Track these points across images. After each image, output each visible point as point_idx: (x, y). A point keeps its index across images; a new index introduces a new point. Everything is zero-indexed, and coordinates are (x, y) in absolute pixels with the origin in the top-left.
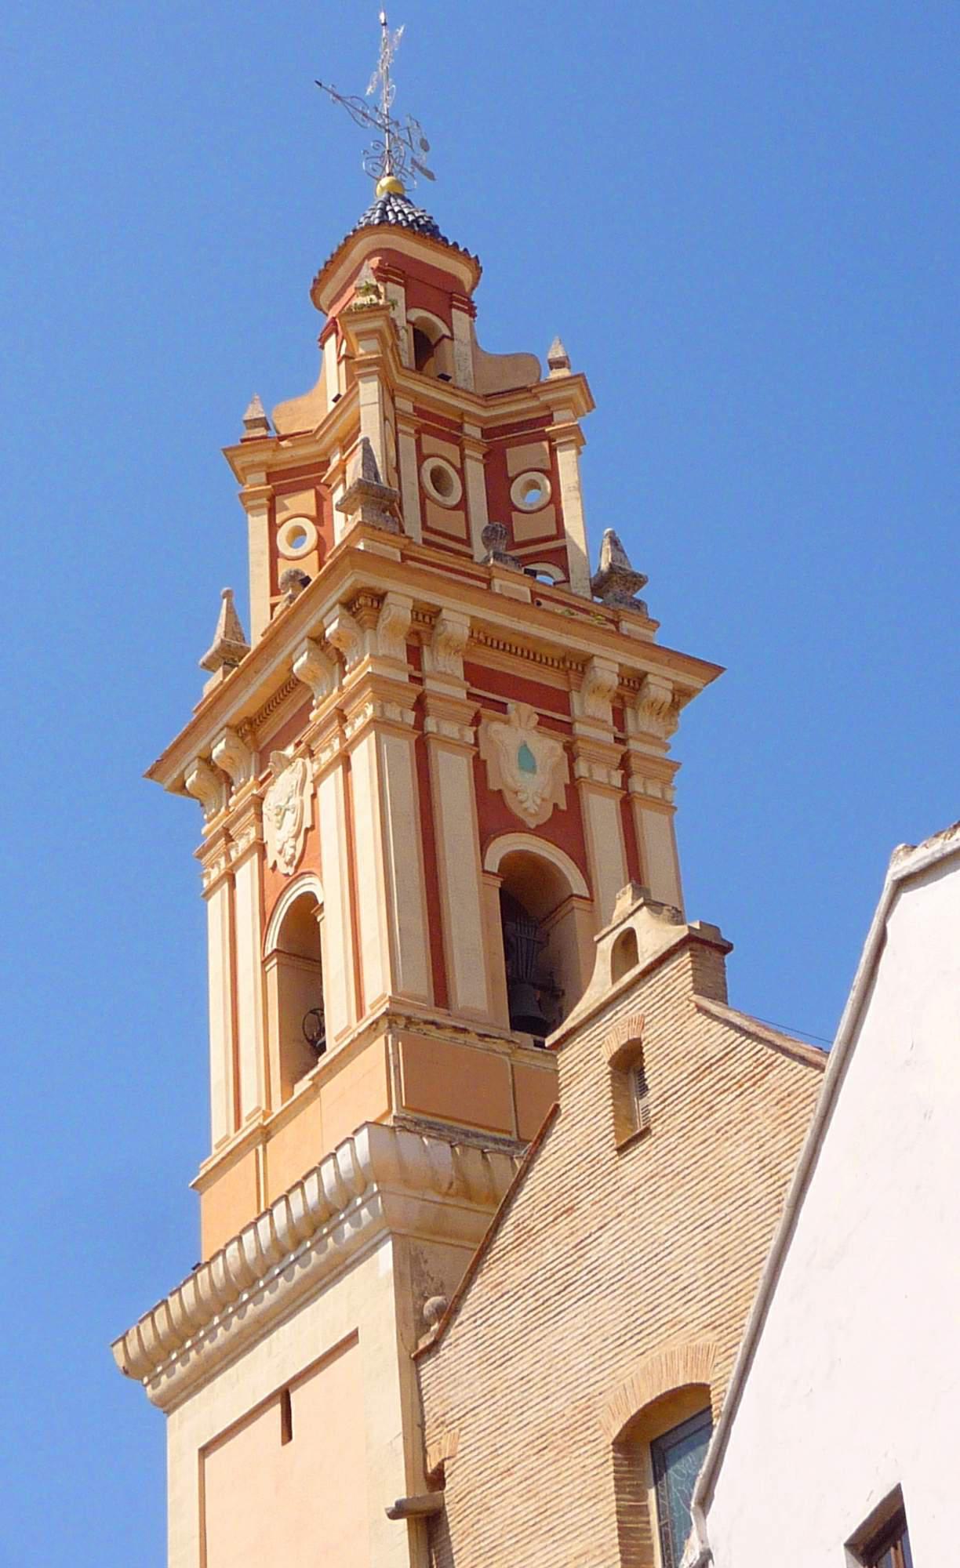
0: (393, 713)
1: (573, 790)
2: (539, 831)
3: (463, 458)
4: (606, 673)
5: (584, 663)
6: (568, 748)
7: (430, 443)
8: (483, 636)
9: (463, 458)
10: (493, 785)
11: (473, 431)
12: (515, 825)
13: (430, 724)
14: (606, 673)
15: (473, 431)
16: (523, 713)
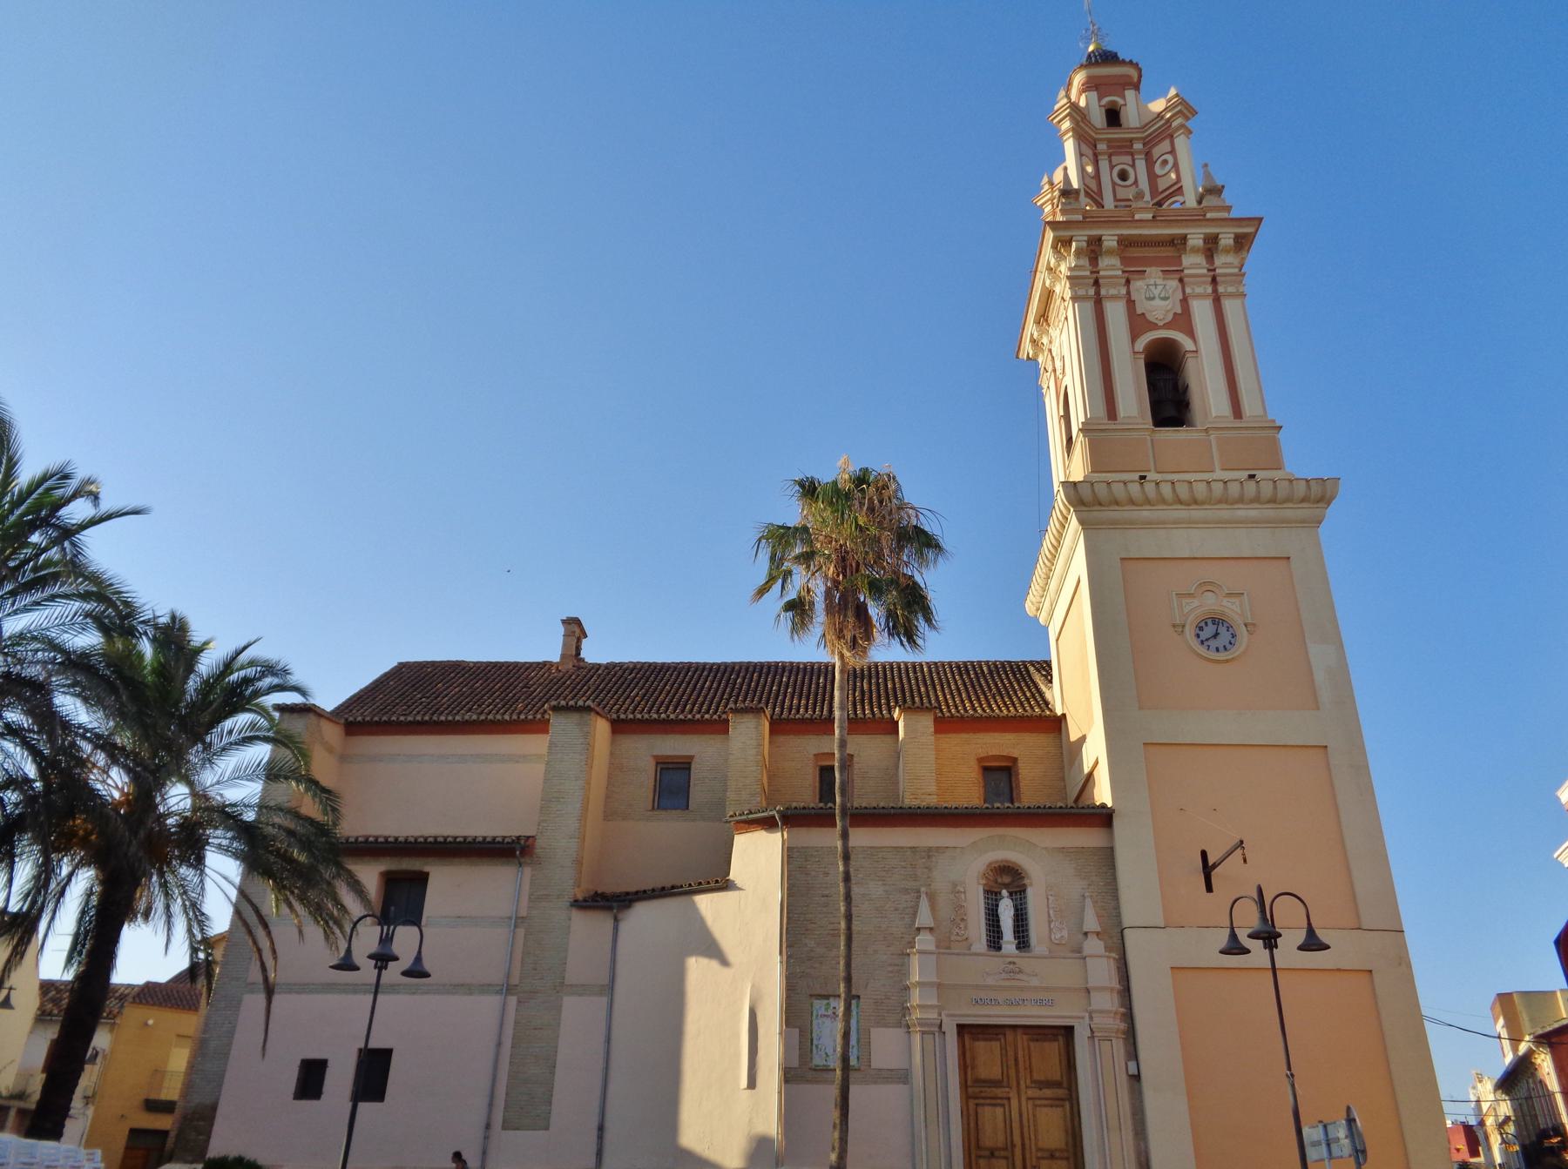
0: (1081, 292)
1: (1185, 301)
2: (1167, 326)
4: (1196, 239)
5: (1184, 238)
6: (1181, 280)
7: (1115, 159)
8: (1126, 243)
10: (1139, 311)
11: (1138, 146)
12: (1154, 326)
13: (1103, 292)
14: (1196, 239)
15: (1138, 146)
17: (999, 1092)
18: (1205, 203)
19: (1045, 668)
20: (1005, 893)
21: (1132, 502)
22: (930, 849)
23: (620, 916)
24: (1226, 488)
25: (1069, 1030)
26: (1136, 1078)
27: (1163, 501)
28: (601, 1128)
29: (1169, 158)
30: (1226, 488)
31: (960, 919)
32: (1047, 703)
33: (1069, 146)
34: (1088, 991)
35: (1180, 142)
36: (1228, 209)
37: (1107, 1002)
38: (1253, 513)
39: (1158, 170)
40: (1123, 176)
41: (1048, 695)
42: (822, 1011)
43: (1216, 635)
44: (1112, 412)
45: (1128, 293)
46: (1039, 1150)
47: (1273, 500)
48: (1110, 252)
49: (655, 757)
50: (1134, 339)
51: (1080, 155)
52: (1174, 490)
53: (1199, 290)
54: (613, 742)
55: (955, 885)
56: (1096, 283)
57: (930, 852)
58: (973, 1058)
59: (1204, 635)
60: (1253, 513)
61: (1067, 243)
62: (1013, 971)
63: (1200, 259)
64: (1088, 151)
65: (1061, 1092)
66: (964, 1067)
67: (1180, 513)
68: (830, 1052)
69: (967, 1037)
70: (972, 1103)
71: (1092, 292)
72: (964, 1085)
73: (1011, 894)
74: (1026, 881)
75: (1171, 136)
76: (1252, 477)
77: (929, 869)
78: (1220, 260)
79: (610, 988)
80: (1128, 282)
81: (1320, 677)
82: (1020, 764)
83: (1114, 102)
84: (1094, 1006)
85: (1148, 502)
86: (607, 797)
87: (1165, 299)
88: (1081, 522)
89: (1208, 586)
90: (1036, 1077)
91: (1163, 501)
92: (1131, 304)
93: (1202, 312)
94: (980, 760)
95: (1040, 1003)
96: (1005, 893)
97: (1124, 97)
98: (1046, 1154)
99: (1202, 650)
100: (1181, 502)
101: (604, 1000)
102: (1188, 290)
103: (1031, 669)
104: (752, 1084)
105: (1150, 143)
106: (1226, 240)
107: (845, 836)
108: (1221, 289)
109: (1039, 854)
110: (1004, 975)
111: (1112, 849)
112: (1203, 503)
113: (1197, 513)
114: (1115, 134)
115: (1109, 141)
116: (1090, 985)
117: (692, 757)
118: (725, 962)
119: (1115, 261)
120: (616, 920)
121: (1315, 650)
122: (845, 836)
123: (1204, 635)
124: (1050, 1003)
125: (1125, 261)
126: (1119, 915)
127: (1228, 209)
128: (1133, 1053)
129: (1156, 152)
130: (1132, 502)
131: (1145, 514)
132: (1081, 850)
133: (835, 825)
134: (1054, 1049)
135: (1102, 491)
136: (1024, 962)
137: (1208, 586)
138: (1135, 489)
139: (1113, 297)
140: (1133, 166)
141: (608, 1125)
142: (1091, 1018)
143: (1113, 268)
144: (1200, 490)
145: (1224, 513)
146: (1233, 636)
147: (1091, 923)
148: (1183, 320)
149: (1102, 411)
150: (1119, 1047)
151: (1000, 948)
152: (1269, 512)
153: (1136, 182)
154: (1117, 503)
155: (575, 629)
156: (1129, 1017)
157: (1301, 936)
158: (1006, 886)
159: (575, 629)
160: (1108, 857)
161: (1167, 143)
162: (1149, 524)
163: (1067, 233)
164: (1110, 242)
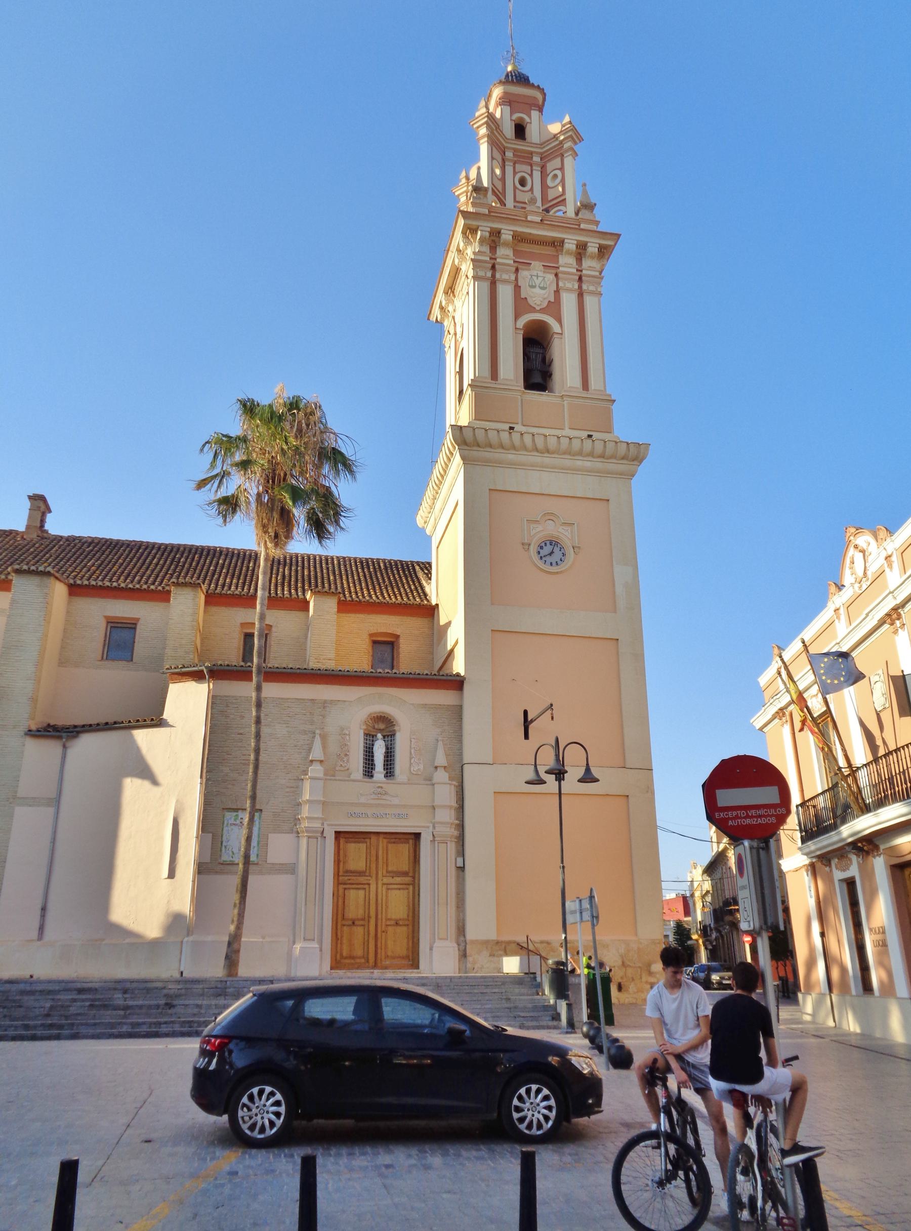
0: (481, 273)
1: (557, 292)
2: (542, 311)
3: (532, 171)
4: (570, 246)
5: (562, 242)
6: (556, 275)
7: (519, 167)
9: (532, 171)
10: (523, 296)
11: (536, 159)
12: (533, 310)
14: (570, 246)
15: (536, 159)
16: (537, 265)
17: (362, 879)
18: (580, 216)
19: (427, 567)
20: (379, 736)
21: (502, 446)
22: (325, 702)
23: (68, 744)
24: (570, 443)
25: (417, 836)
26: (462, 869)
27: (525, 448)
28: (44, 909)
29: (558, 173)
30: (570, 443)
31: (344, 754)
32: (425, 595)
33: (484, 148)
34: (434, 808)
35: (568, 161)
36: (597, 223)
37: (447, 816)
38: (588, 464)
39: (550, 183)
40: (523, 182)
41: (427, 589)
42: (232, 821)
43: (551, 553)
44: (494, 375)
45: (516, 279)
46: (387, 919)
47: (602, 456)
48: (506, 244)
49: (106, 617)
50: (517, 317)
51: (492, 158)
52: (533, 440)
53: (569, 285)
54: (69, 603)
55: (342, 729)
56: (493, 267)
57: (325, 704)
58: (345, 856)
59: (543, 553)
60: (588, 464)
61: (474, 231)
62: (381, 793)
63: (572, 261)
64: (498, 156)
65: (407, 879)
66: (338, 862)
67: (537, 459)
68: (235, 851)
69: (342, 841)
70: (341, 887)
71: (489, 274)
72: (337, 875)
73: (384, 737)
74: (396, 728)
75: (562, 155)
76: (590, 436)
77: (324, 716)
78: (586, 263)
79: (56, 802)
80: (517, 270)
81: (619, 589)
82: (401, 640)
83: (521, 119)
84: (437, 819)
85: (514, 447)
86: (62, 647)
87: (543, 288)
88: (463, 458)
89: (550, 516)
90: (390, 869)
91: (525, 448)
92: (517, 288)
93: (569, 302)
94: (371, 635)
95: (399, 816)
96: (379, 736)
97: (530, 117)
98: (393, 922)
99: (540, 563)
100: (537, 450)
101: (51, 810)
102: (561, 284)
103: (417, 568)
104: (172, 874)
105: (545, 158)
106: (593, 249)
107: (259, 688)
108: (584, 287)
109: (407, 708)
110: (373, 796)
111: (461, 707)
112: (553, 453)
113: (547, 460)
114: (520, 145)
115: (515, 150)
116: (435, 804)
117: (138, 619)
118: (155, 782)
119: (509, 252)
120: (64, 746)
121: (618, 569)
122: (259, 688)
123: (543, 553)
124: (406, 817)
125: (516, 252)
126: (461, 755)
127: (597, 223)
128: (461, 852)
129: (550, 166)
130: (502, 446)
131: (510, 457)
132: (438, 707)
133: (251, 680)
134: (405, 849)
135: (480, 435)
136: (390, 786)
137: (550, 516)
138: (505, 436)
139: (505, 282)
140: (531, 175)
141: (50, 906)
142: (434, 827)
143: (506, 257)
144: (552, 442)
145: (567, 462)
146: (564, 555)
147: (441, 759)
148: (554, 307)
149: (487, 373)
150: (452, 847)
151: (372, 776)
152: (598, 464)
153: (532, 190)
154: (491, 446)
155: (40, 505)
156: (461, 827)
157: (581, 772)
158: (381, 731)
159: (40, 505)
160: (458, 712)
161: (559, 159)
162: (513, 465)
163: (474, 223)
164: (507, 236)
